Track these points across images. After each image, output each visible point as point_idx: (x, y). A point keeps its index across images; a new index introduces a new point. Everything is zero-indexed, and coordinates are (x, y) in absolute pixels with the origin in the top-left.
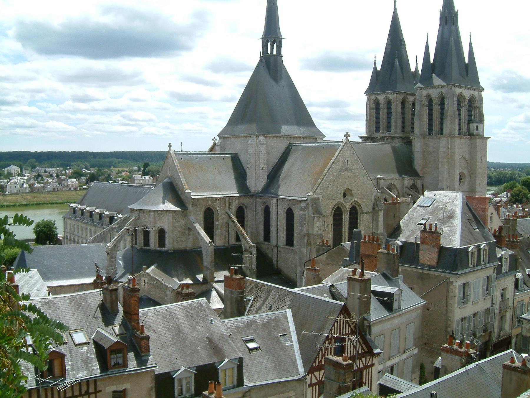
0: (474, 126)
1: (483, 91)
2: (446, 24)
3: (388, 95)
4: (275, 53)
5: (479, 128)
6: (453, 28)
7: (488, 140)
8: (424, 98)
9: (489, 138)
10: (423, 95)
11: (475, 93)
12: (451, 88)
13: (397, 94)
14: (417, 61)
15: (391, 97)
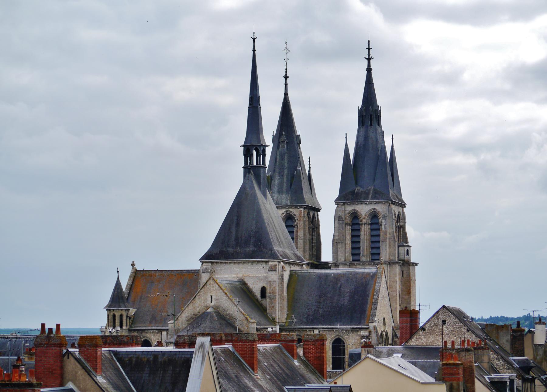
0: (404, 250)
1: (405, 207)
2: (371, 125)
3: (291, 210)
4: (255, 164)
5: (409, 252)
6: (379, 129)
7: (416, 266)
8: (348, 215)
9: (416, 264)
10: (347, 212)
11: (400, 209)
12: (390, 205)
13: (304, 208)
14: (309, 165)
15: (294, 211)
